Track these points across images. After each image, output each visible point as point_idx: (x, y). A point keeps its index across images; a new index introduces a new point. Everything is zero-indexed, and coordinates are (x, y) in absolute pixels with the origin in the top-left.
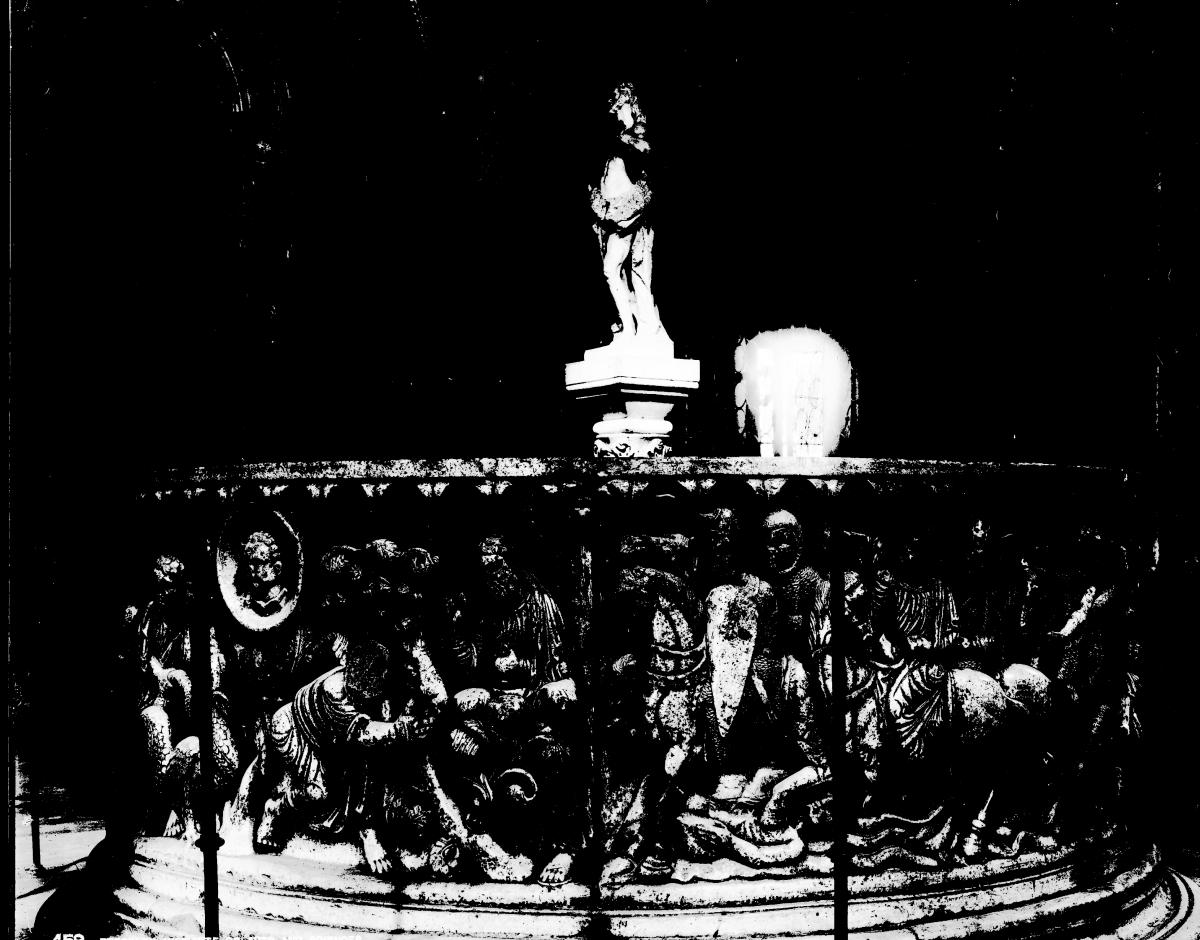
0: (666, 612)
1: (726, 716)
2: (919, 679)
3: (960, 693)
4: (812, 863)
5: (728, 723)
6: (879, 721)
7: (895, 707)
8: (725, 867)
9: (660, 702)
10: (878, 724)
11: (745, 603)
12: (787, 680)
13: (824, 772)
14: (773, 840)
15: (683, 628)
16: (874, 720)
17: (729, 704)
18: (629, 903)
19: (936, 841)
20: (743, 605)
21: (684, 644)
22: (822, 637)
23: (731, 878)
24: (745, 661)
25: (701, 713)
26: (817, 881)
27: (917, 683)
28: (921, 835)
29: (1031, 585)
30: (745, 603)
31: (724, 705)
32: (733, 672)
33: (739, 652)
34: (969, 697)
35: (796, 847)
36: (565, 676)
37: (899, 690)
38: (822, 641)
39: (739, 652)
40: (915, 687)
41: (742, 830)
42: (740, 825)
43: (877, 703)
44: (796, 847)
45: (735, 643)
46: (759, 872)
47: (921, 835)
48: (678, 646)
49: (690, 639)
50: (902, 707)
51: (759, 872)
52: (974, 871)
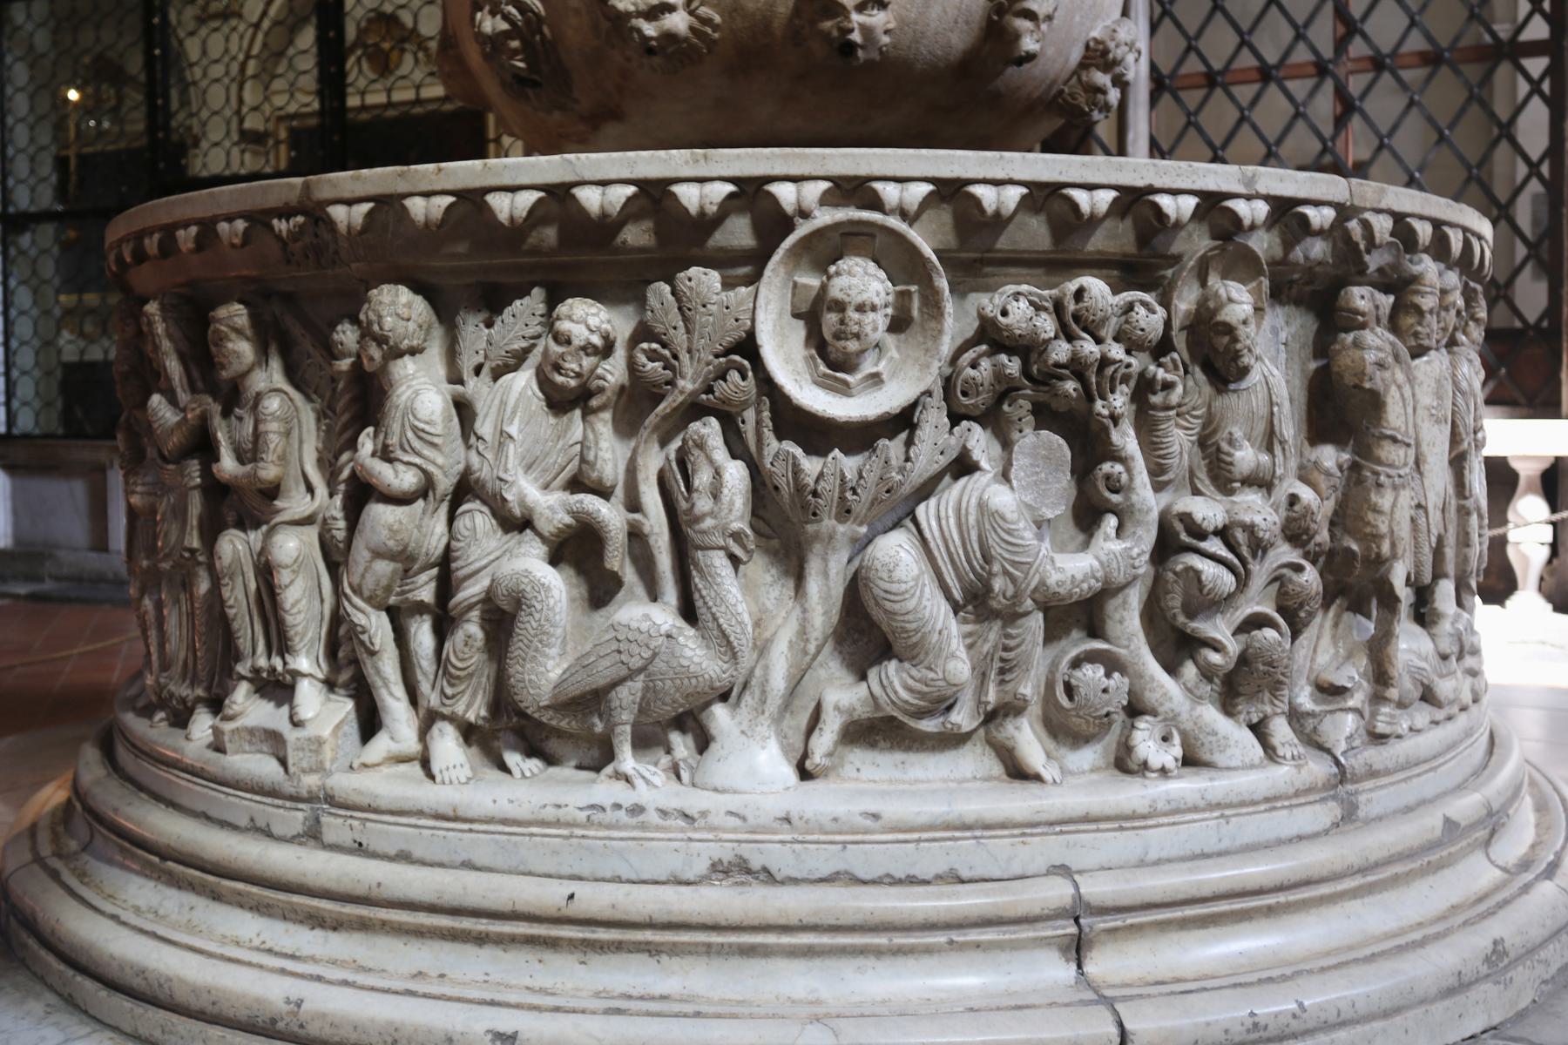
0: (1399, 387)
18: (1373, 774)
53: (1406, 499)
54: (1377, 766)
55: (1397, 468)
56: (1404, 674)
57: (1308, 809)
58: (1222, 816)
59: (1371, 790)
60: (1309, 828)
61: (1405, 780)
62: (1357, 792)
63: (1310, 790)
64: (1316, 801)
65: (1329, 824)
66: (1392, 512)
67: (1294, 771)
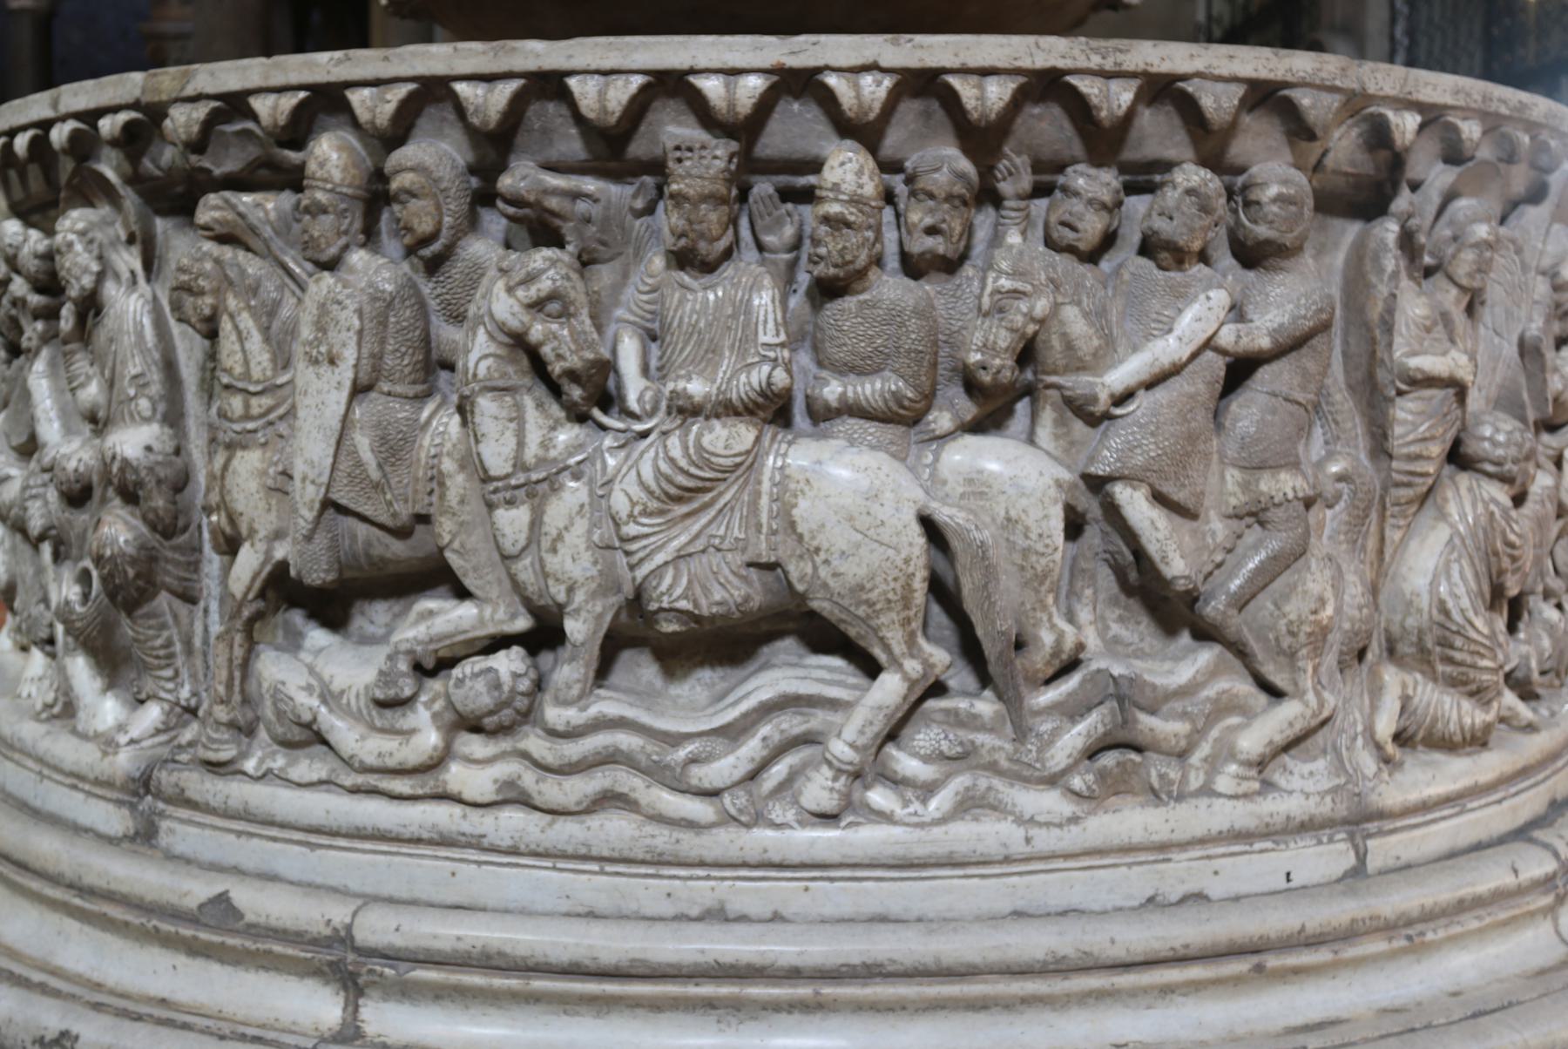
0: (232, 317)
1: (307, 499)
2: (676, 451)
3: (792, 486)
4: (457, 776)
5: (311, 509)
6: (594, 525)
7: (620, 503)
8: (309, 767)
9: (225, 467)
10: (590, 532)
11: (339, 303)
12: (426, 442)
13: (494, 611)
14: (387, 725)
15: (255, 342)
16: (581, 526)
17: (311, 476)
19: (726, 767)
20: (336, 307)
21: (256, 373)
22: (471, 365)
23: (321, 782)
24: (337, 400)
25: (280, 485)
26: (457, 810)
27: (672, 461)
28: (682, 753)
29: (996, 280)
30: (339, 303)
31: (304, 479)
32: (318, 422)
33: (326, 387)
34: (809, 494)
35: (429, 739)
36: (147, 420)
37: (633, 472)
38: (471, 372)
39: (326, 387)
40: (664, 467)
41: (344, 701)
42: (342, 692)
43: (591, 493)
44: (429, 739)
45: (322, 371)
46: (360, 779)
47: (682, 753)
48: (247, 375)
49: (265, 364)
50: (633, 504)
51: (360, 779)
52: (823, 839)
53: (248, 465)
54: (191, 793)
55: (231, 420)
56: (267, 696)
57: (102, 804)
58: (40, 773)
59: (182, 821)
60: (103, 828)
61: (239, 834)
62: (162, 814)
63: (108, 784)
64: (109, 800)
65: (120, 834)
66: (223, 477)
67: (99, 754)
